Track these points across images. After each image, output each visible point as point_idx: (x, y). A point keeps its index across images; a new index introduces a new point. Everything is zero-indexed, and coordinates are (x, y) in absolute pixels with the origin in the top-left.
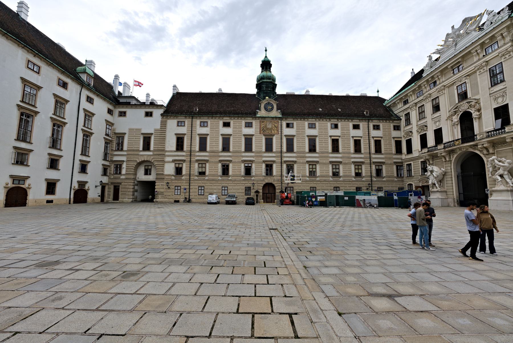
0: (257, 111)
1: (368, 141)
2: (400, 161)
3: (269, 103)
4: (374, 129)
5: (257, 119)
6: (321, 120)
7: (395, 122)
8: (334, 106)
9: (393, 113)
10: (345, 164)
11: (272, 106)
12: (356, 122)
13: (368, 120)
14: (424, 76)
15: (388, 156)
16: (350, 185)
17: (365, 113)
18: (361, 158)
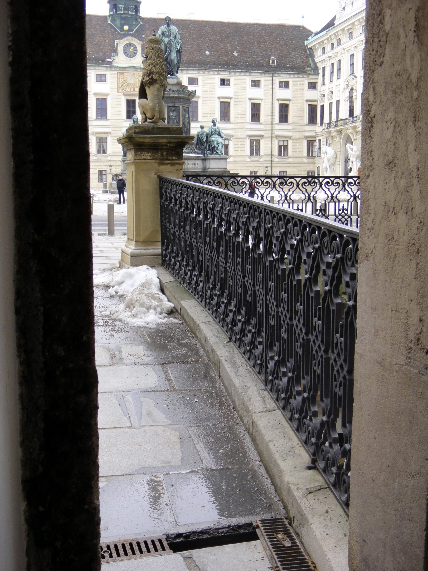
0: (112, 54)
1: (270, 105)
2: (313, 134)
3: (130, 44)
4: (281, 87)
5: (113, 69)
6: (206, 73)
7: (310, 76)
8: (229, 45)
9: (313, 61)
10: (237, 138)
11: (135, 49)
12: (256, 76)
13: (273, 73)
14: (336, 24)
15: (298, 127)
16: (242, 168)
17: (271, 61)
18: (259, 130)
